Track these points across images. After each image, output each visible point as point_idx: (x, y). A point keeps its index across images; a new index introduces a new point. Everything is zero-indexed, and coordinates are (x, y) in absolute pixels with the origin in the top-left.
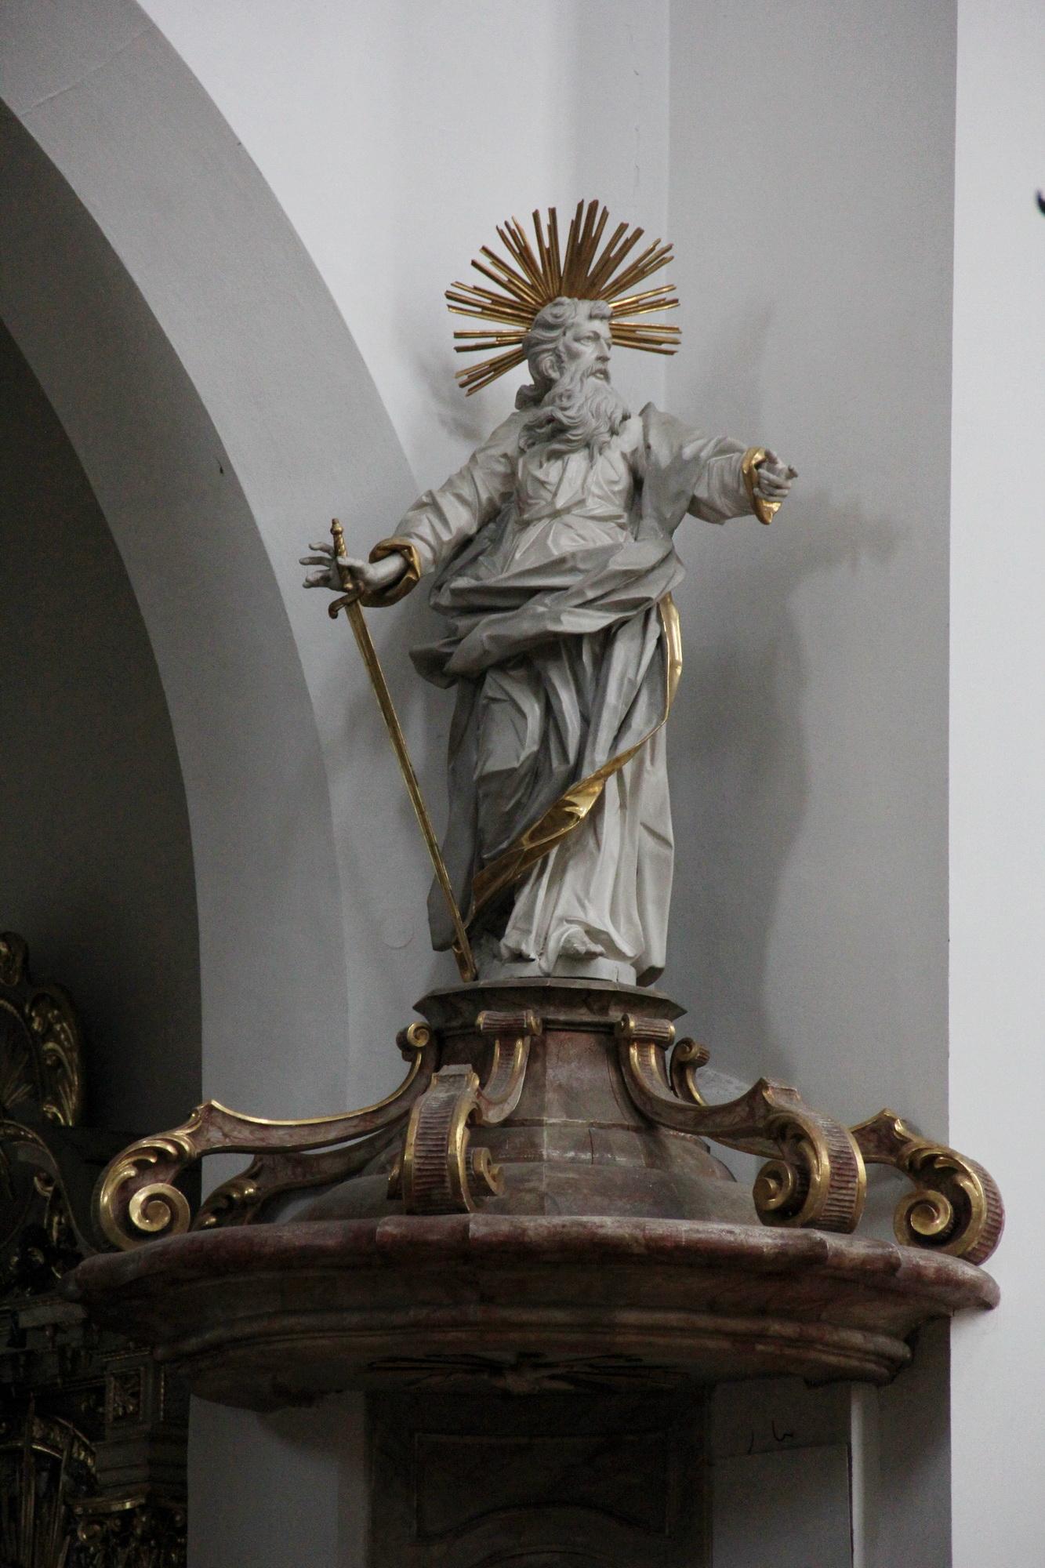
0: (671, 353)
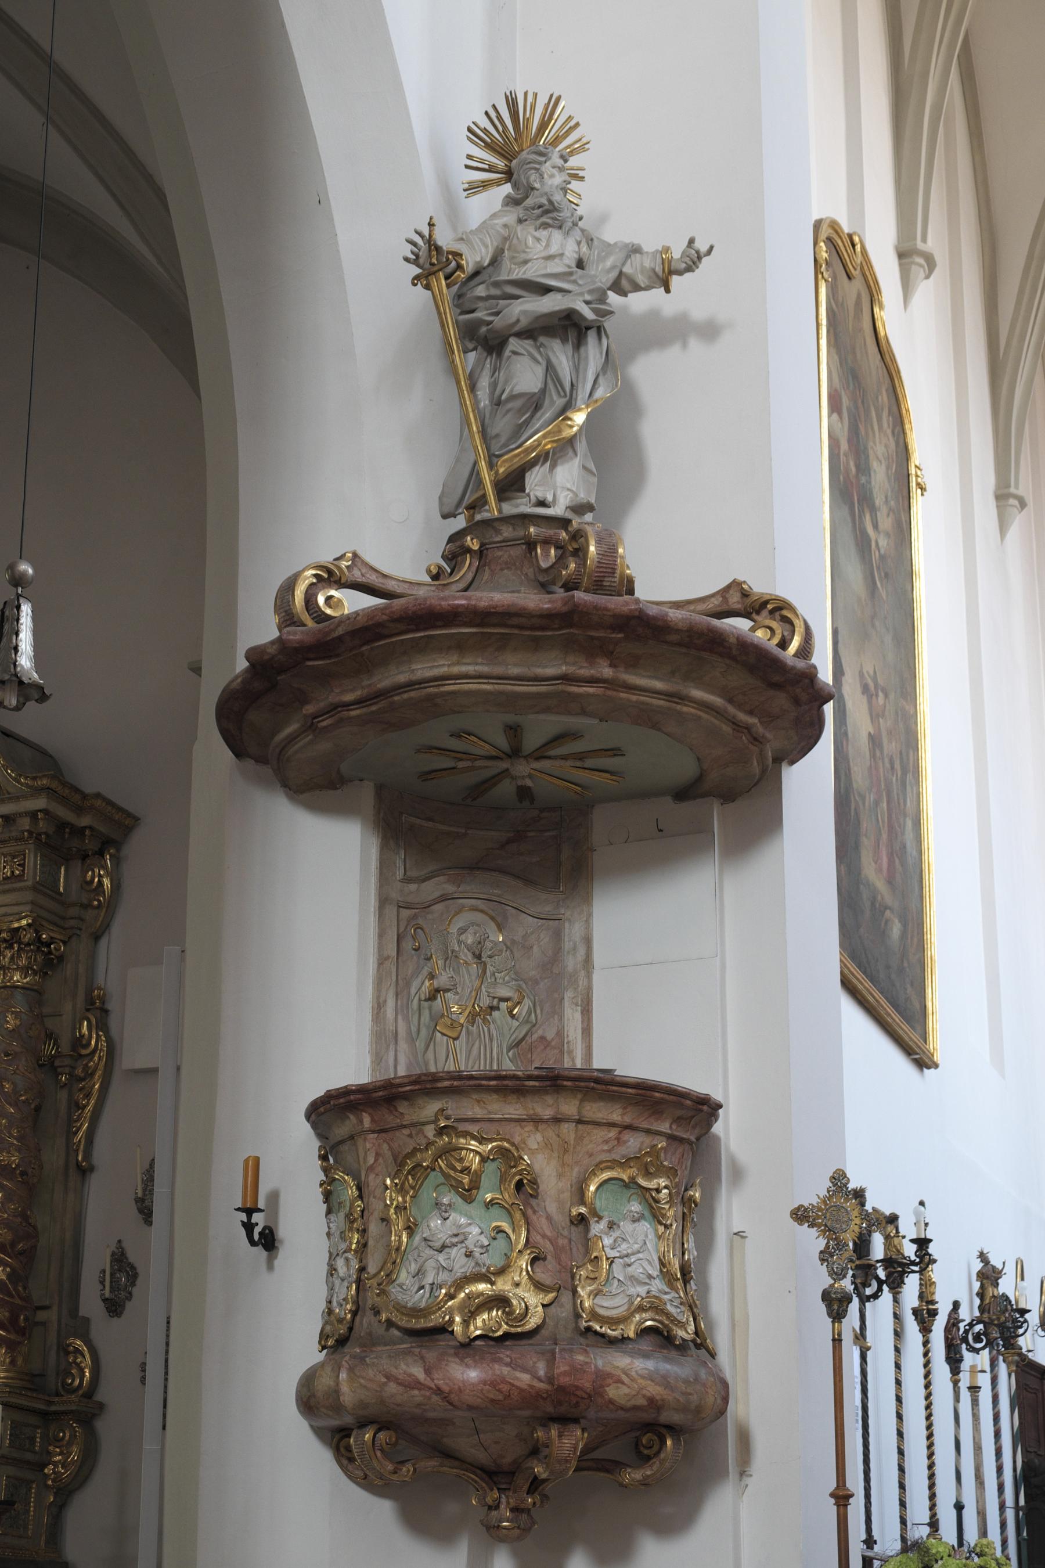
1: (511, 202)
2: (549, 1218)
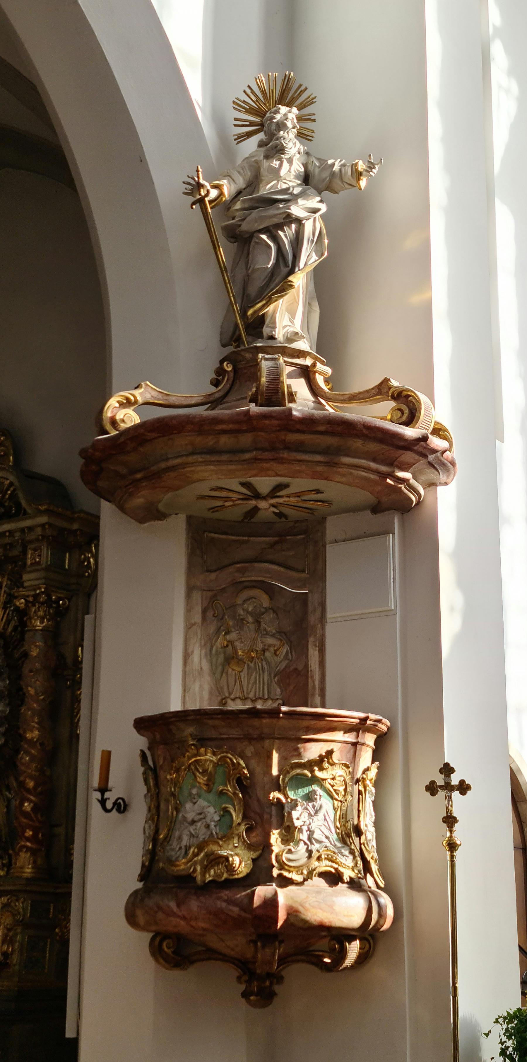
0: (311, 140)
1: (261, 144)
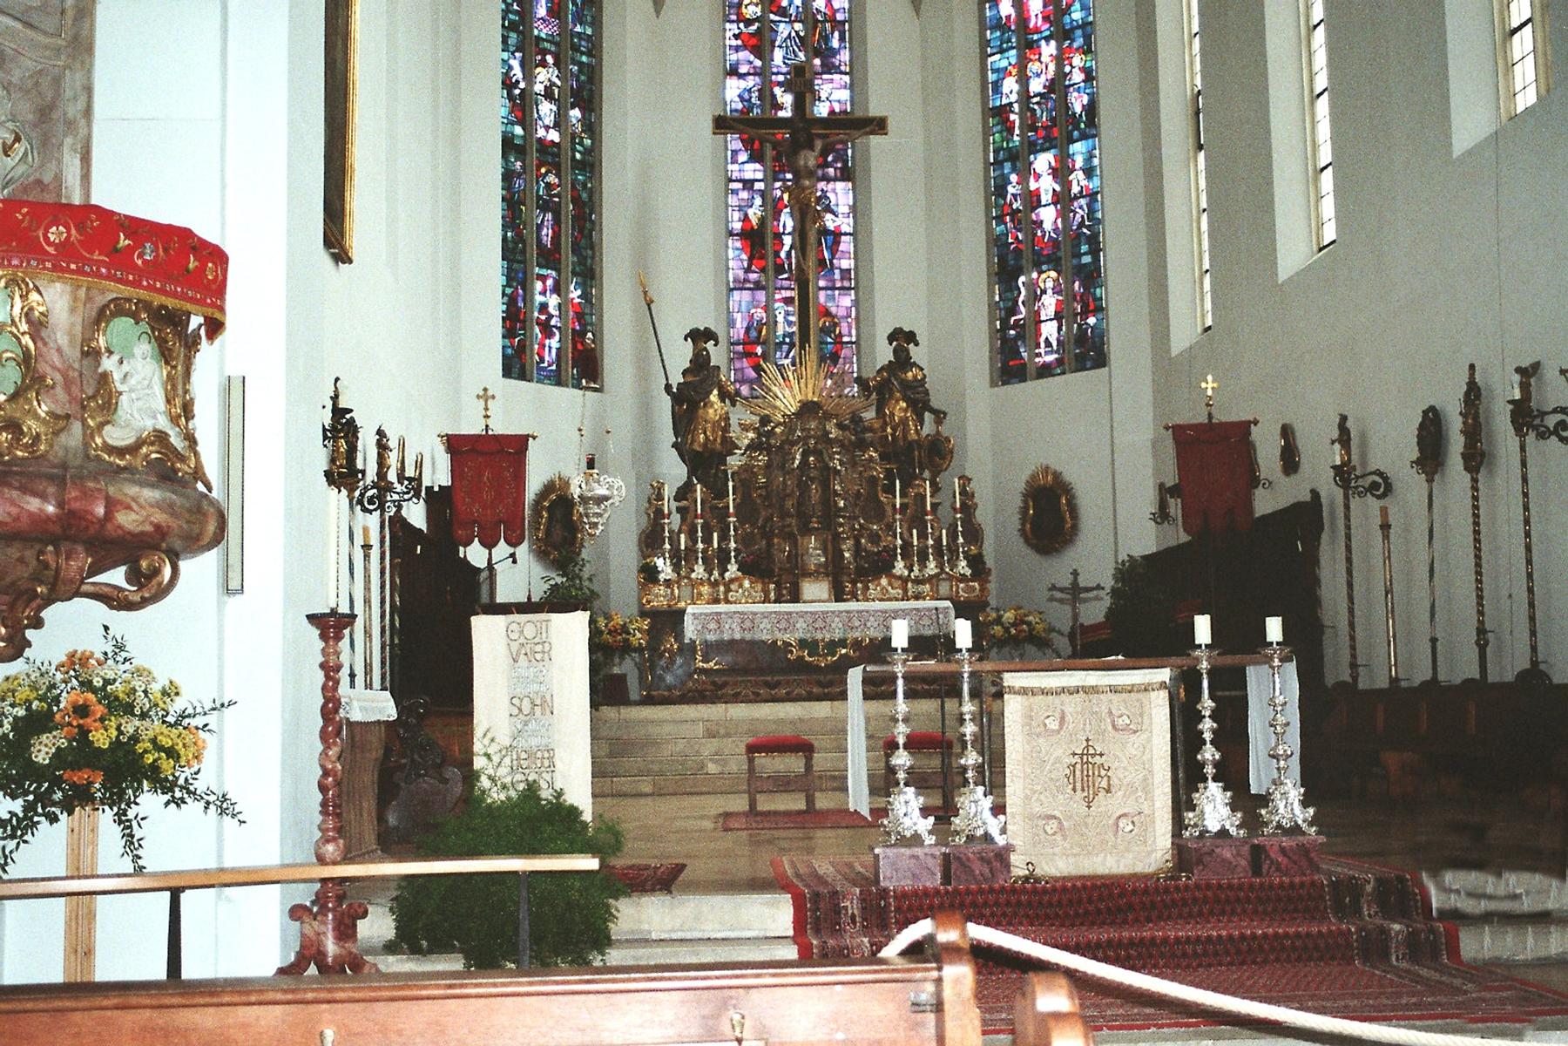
2: (59, 350)
